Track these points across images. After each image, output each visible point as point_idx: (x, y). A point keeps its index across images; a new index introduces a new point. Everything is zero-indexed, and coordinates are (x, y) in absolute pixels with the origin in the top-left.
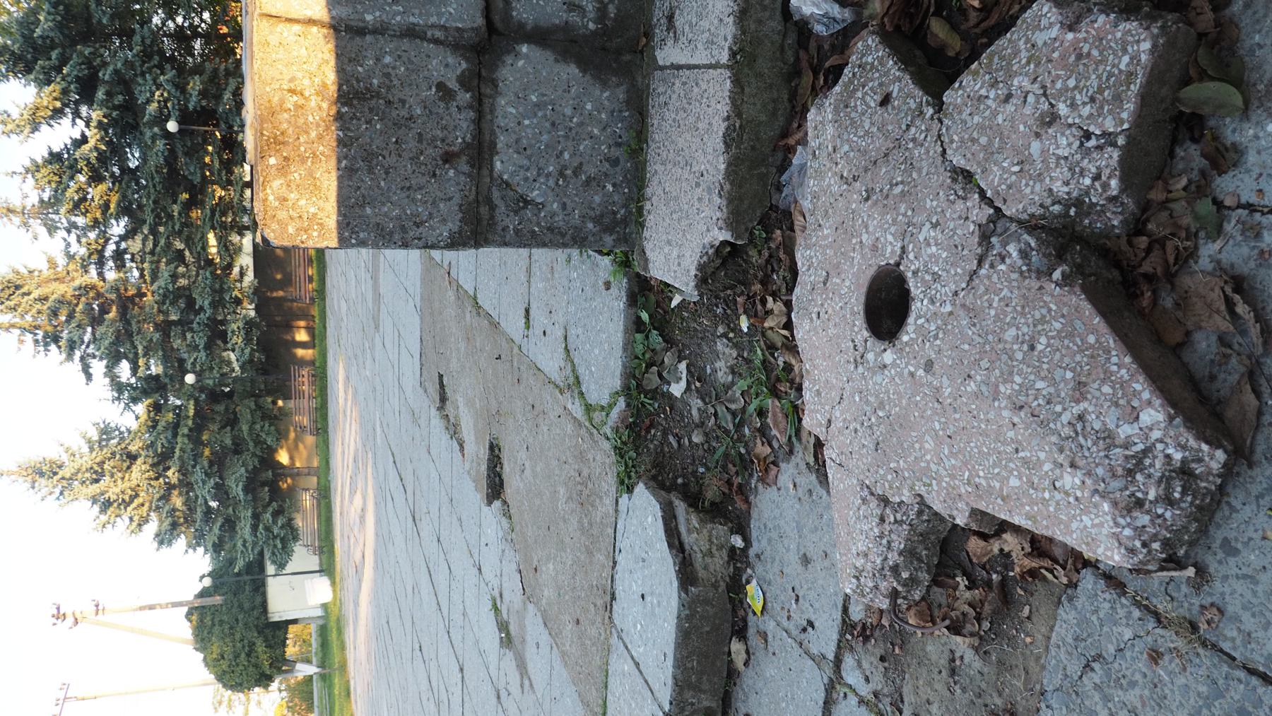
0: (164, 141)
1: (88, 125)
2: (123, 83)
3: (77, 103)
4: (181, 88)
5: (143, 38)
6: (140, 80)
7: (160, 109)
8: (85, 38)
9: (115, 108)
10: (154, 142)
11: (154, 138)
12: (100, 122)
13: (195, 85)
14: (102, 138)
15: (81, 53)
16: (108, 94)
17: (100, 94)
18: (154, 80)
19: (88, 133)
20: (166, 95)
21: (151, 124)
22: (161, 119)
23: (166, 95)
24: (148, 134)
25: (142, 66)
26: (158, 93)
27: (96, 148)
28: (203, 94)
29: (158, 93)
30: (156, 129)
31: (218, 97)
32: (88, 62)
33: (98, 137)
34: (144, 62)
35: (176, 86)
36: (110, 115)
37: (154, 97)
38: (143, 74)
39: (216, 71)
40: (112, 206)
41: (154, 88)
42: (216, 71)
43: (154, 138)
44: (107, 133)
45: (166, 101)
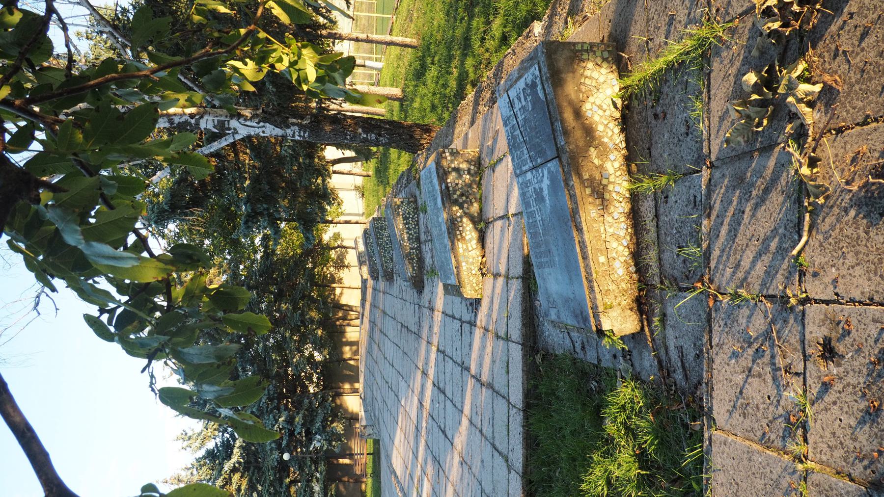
11: (271, 450)
40: (243, 487)
45: (281, 429)
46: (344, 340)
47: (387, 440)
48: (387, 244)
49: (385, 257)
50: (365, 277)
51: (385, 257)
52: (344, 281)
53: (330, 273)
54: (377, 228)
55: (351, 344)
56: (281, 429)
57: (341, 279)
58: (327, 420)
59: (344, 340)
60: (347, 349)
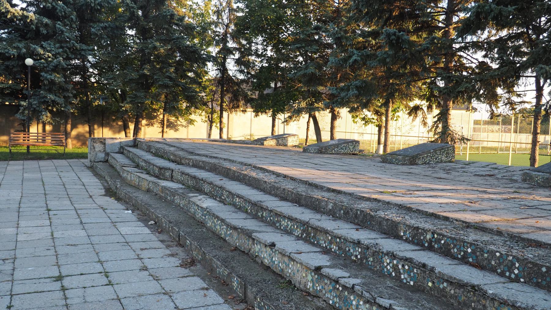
0: (16, 54)
1: (22, 9)
2: (53, 35)
3: (38, 6)
4: (56, 69)
5: (85, 50)
6: (58, 45)
7: (40, 55)
8: (81, 17)
9: (37, 27)
10: (15, 48)
11: (17, 48)
12: (27, 17)
13: (58, 78)
14: (15, 17)
15: (72, 14)
16: (46, 25)
17: (46, 20)
18: (59, 54)
19: (18, 9)
20: (50, 59)
21: (28, 48)
22: (32, 55)
23: (50, 59)
24: (20, 45)
25: (67, 47)
26: (50, 55)
27: (8, 12)
28: (52, 82)
29: (50, 55)
30: (24, 50)
31: (50, 91)
32: (65, 17)
33: (16, 14)
34: (69, 49)
35: (56, 67)
36: (32, 24)
37: (47, 51)
38: (61, 47)
39: (67, 90)
41: (53, 53)
42: (67, 90)
43: (17, 48)
44: (20, 20)
46: (96, 127)
47: (316, 161)
48: (436, 159)
49: (427, 157)
50: (265, 143)
51: (427, 157)
52: (151, 128)
53: (157, 116)
54: (448, 150)
55: (91, 132)
56: (46, 59)
57: (152, 125)
58: (53, 106)
59: (96, 127)
60: (87, 129)
